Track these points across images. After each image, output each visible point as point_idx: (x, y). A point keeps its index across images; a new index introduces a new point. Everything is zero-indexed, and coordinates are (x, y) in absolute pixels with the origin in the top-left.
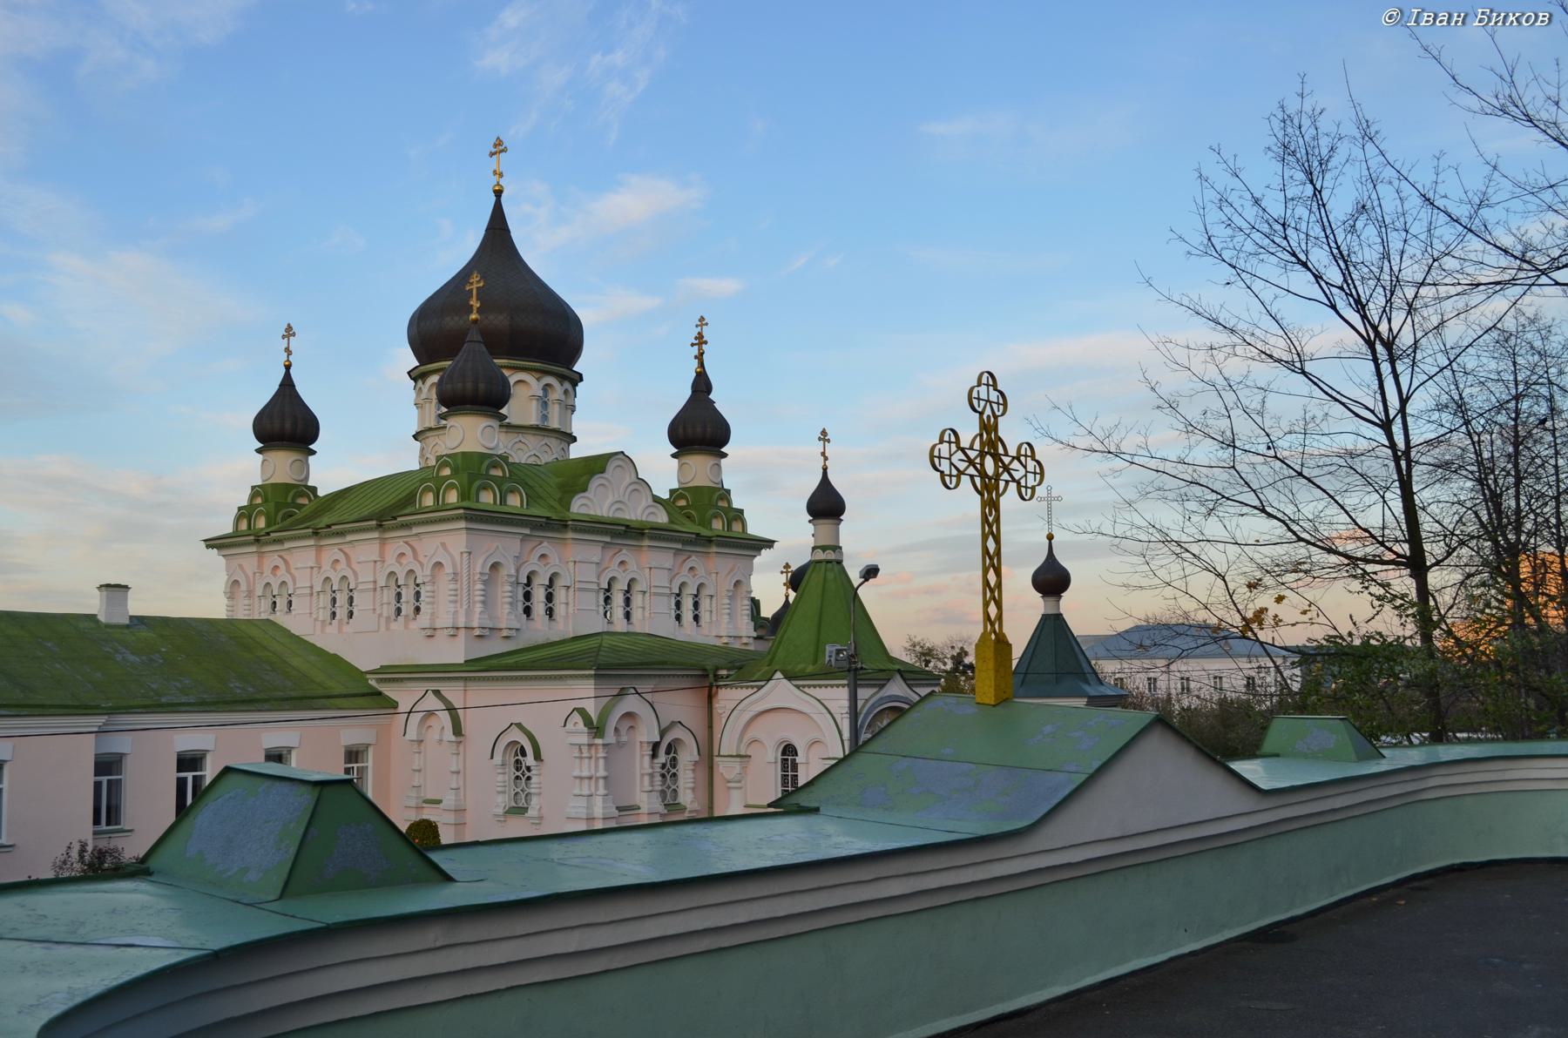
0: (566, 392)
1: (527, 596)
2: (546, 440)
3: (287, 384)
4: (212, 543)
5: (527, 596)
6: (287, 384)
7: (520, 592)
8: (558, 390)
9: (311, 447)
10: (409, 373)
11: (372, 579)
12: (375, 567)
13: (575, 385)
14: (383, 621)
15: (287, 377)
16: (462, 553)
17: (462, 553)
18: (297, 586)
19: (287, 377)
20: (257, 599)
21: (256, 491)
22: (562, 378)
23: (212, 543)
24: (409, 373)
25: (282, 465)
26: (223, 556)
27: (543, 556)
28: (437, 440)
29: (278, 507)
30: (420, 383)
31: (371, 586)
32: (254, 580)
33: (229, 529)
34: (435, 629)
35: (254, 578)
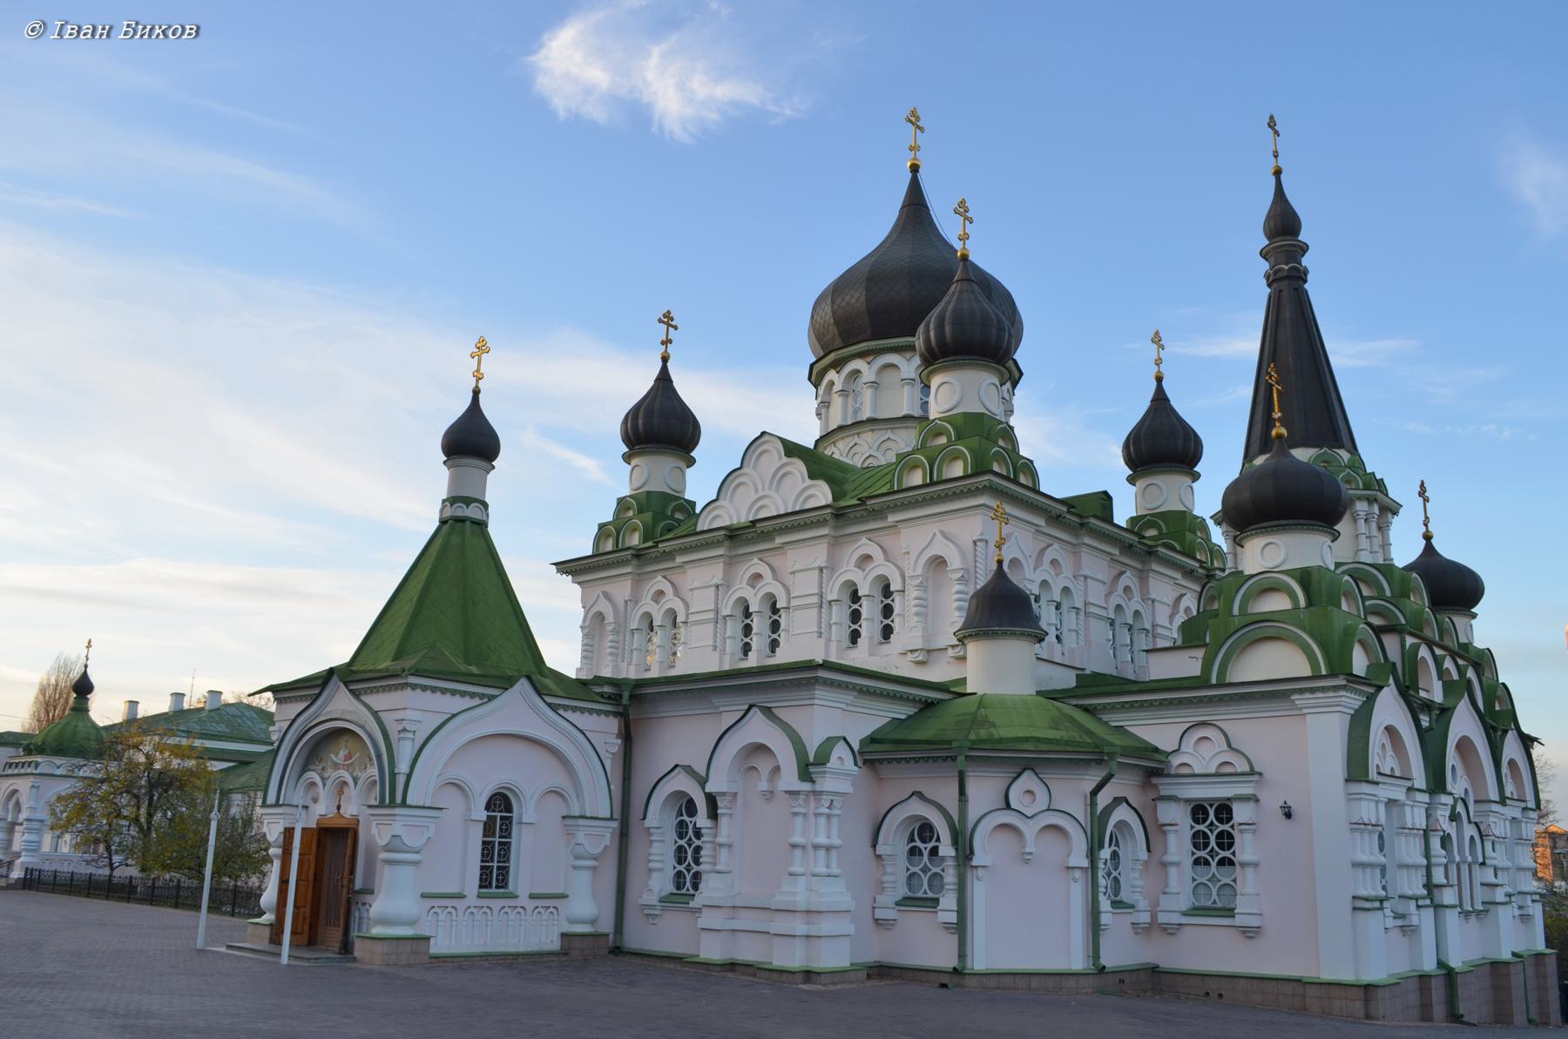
4: (565, 567)
11: (816, 591)
12: (821, 577)
16: (975, 542)
17: (975, 542)
18: (691, 611)
20: (628, 634)
21: (622, 504)
23: (565, 567)
25: (657, 471)
26: (579, 583)
28: (856, 439)
29: (659, 516)
30: (832, 375)
32: (626, 609)
33: (587, 550)
34: (929, 651)
35: (626, 609)
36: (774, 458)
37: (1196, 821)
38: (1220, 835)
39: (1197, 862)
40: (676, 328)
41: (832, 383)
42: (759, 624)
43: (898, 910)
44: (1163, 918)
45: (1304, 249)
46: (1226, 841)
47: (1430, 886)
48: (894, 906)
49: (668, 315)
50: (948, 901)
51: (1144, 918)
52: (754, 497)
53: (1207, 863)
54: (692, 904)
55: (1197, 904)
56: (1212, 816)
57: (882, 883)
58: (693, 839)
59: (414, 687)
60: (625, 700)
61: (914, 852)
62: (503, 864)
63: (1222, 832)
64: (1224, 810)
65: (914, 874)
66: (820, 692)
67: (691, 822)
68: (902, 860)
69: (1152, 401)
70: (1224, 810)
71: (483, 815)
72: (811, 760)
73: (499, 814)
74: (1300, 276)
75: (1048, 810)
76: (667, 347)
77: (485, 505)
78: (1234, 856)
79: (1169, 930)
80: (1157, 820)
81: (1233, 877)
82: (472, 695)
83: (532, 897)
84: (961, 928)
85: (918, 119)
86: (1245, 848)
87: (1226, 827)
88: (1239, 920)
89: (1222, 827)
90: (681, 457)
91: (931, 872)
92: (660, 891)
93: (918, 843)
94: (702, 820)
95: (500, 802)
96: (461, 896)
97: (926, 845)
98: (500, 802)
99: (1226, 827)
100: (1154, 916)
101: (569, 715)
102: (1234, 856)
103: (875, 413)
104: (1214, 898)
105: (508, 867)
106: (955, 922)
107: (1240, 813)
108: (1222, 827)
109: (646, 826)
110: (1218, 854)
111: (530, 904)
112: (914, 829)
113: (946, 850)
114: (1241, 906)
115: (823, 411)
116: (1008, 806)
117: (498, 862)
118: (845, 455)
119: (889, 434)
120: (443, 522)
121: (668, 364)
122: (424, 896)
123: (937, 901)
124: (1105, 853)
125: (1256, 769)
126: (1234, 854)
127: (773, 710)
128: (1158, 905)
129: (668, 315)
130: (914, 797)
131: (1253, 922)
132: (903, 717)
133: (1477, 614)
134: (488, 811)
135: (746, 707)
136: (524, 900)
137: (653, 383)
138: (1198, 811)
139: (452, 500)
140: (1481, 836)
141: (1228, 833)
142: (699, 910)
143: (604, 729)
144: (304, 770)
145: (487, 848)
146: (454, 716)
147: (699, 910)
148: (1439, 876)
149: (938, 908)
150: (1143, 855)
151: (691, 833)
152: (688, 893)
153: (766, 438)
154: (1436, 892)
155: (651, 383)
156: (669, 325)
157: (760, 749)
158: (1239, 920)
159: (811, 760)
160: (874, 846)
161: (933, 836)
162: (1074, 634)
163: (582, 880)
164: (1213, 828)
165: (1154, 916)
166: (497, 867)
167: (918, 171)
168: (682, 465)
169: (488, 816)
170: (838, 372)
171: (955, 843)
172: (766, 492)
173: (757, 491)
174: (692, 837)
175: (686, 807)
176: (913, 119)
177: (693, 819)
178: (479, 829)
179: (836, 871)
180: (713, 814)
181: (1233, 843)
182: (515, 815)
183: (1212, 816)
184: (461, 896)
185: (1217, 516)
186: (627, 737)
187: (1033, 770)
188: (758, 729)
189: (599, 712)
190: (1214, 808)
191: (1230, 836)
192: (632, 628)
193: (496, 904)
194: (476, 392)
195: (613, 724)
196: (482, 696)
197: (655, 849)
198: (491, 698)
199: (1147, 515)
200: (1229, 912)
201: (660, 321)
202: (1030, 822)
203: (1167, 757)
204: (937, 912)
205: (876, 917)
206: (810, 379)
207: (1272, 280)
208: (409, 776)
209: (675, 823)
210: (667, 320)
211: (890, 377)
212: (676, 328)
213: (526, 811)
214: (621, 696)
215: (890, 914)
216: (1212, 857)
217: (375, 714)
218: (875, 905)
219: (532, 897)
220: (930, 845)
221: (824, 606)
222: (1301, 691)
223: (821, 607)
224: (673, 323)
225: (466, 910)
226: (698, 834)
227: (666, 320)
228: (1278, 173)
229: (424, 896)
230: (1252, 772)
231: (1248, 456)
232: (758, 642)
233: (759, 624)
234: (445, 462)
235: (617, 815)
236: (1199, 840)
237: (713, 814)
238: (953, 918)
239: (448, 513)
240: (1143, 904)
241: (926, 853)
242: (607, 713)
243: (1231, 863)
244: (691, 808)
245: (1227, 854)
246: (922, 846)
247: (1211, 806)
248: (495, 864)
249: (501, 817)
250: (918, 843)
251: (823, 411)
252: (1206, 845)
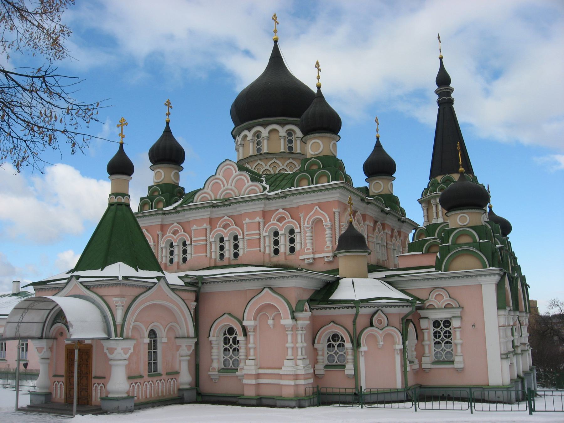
9: (181, 165)
28: (259, 162)
30: (246, 132)
31: (258, 237)
37: (435, 327)
38: (445, 332)
39: (436, 343)
40: (171, 107)
41: (246, 136)
43: (325, 371)
44: (424, 366)
45: (452, 90)
46: (448, 334)
47: (513, 346)
48: (323, 369)
50: (350, 367)
51: (417, 367)
52: (223, 189)
53: (440, 343)
54: (237, 373)
55: (436, 360)
56: (442, 325)
57: (317, 359)
58: (232, 344)
60: (200, 285)
61: (329, 346)
62: (155, 361)
63: (446, 331)
64: (447, 323)
65: (331, 355)
67: (231, 338)
68: (326, 350)
69: (375, 147)
70: (447, 323)
72: (294, 309)
73: (152, 339)
74: (451, 102)
75: (388, 326)
76: (168, 116)
77: (129, 196)
78: (452, 340)
79: (424, 370)
80: (420, 327)
81: (451, 349)
83: (168, 374)
84: (356, 376)
86: (457, 337)
87: (448, 329)
88: (456, 366)
89: (446, 329)
90: (177, 169)
91: (338, 354)
92: (219, 368)
93: (332, 342)
95: (152, 334)
96: (141, 377)
97: (336, 343)
99: (448, 329)
100: (420, 365)
101: (178, 293)
102: (452, 340)
103: (268, 150)
104: (443, 357)
105: (157, 362)
106: (353, 374)
107: (455, 323)
108: (446, 329)
109: (210, 340)
110: (444, 340)
112: (330, 338)
113: (348, 345)
114: (457, 359)
115: (241, 148)
116: (372, 325)
117: (153, 360)
118: (253, 168)
119: (274, 160)
120: (111, 205)
121: (169, 124)
123: (344, 366)
124: (407, 343)
125: (461, 305)
126: (451, 339)
127: (273, 289)
128: (422, 361)
130: (332, 322)
131: (461, 366)
132: (319, 289)
133: (509, 238)
134: (150, 338)
135: (263, 288)
137: (162, 133)
138: (436, 323)
139: (114, 194)
140: (521, 325)
141: (448, 331)
142: (243, 376)
146: (137, 297)
148: (516, 344)
149: (345, 369)
150: (416, 342)
151: (231, 342)
152: (231, 368)
153: (228, 162)
154: (516, 349)
155: (161, 133)
156: (169, 106)
158: (456, 366)
159: (294, 309)
160: (313, 343)
161: (339, 338)
164: (442, 329)
165: (420, 365)
166: (153, 362)
167: (277, 42)
168: (178, 172)
169: (150, 340)
170: (249, 132)
171: (352, 342)
172: (229, 187)
173: (224, 186)
174: (232, 344)
175: (228, 331)
176: (275, 18)
177: (233, 336)
179: (305, 357)
180: (245, 334)
181: (451, 335)
182: (158, 339)
183: (442, 325)
184: (141, 377)
185: (420, 200)
186: (197, 300)
187: (381, 310)
190: (442, 322)
191: (450, 333)
192: (162, 246)
193: (154, 379)
197: (215, 351)
199: (376, 195)
200: (452, 362)
201: (166, 104)
202: (381, 332)
203: (424, 302)
204: (344, 371)
205: (316, 374)
206: (231, 133)
207: (439, 103)
208: (123, 326)
209: (223, 338)
211: (274, 136)
212: (171, 107)
214: (198, 283)
215: (322, 372)
216: (442, 341)
217: (101, 297)
218: (315, 369)
219: (168, 374)
220: (338, 343)
221: (261, 238)
222: (481, 275)
223: (260, 239)
224: (171, 105)
225: (144, 383)
226: (236, 342)
227: (168, 104)
228: (441, 59)
230: (460, 307)
231: (433, 174)
234: (109, 177)
236: (437, 335)
237: (245, 334)
238: (352, 373)
239: (115, 200)
240: (416, 361)
241: (336, 347)
242: (191, 291)
243: (450, 343)
244: (231, 331)
245: (449, 340)
246: (334, 343)
247: (441, 321)
248: (152, 362)
249: (153, 340)
250: (332, 342)
251: (241, 148)
252: (439, 337)
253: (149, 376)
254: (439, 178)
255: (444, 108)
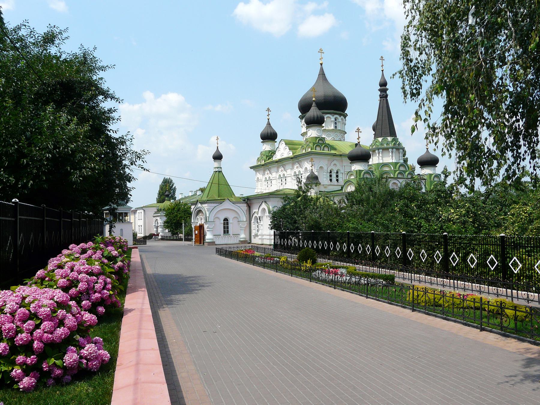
0: (342, 119)
1: (331, 176)
2: (336, 133)
3: (269, 124)
4: (251, 168)
5: (331, 176)
6: (269, 124)
7: (329, 175)
8: (340, 118)
10: (299, 117)
13: (345, 117)
14: (293, 184)
15: (269, 121)
19: (269, 121)
22: (340, 115)
23: (251, 168)
24: (299, 117)
27: (335, 164)
29: (267, 156)
36: (284, 145)
40: (271, 111)
42: (284, 180)
45: (387, 89)
49: (268, 109)
59: (208, 203)
66: (271, 199)
71: (223, 222)
74: (386, 96)
77: (221, 168)
82: (218, 203)
83: (233, 235)
85: (322, 50)
94: (259, 221)
95: (226, 220)
96: (220, 235)
98: (226, 220)
101: (236, 204)
111: (233, 236)
122: (214, 235)
129: (268, 109)
136: (231, 235)
143: (244, 207)
144: (197, 216)
145: (224, 228)
147: (258, 236)
157: (264, 209)
162: (341, 178)
163: (243, 232)
178: (223, 224)
180: (260, 220)
184: (220, 235)
188: (264, 206)
189: (242, 203)
194: (218, 147)
195: (245, 205)
196: (220, 203)
198: (222, 203)
201: (266, 111)
208: (209, 217)
210: (268, 110)
212: (271, 111)
213: (230, 221)
219: (233, 235)
228: (383, 71)
229: (214, 235)
232: (284, 184)
233: (284, 180)
235: (248, 220)
237: (260, 220)
242: (244, 203)
253: (224, 235)
254: (380, 139)
255: (384, 100)
